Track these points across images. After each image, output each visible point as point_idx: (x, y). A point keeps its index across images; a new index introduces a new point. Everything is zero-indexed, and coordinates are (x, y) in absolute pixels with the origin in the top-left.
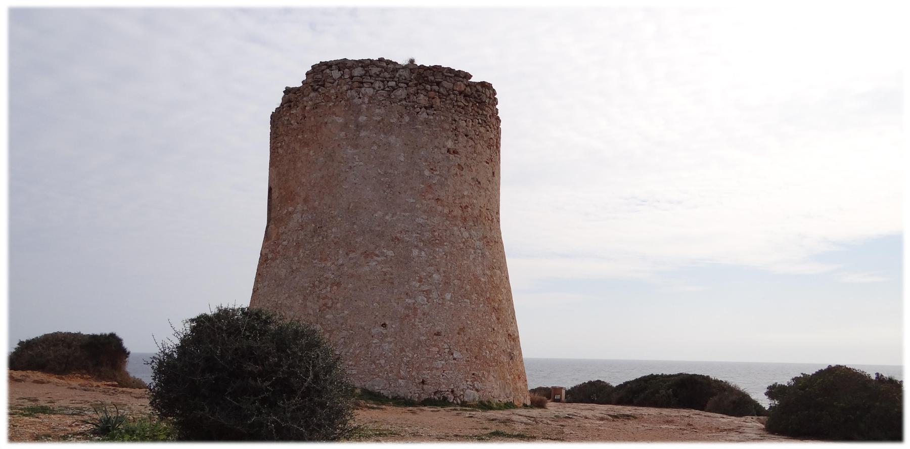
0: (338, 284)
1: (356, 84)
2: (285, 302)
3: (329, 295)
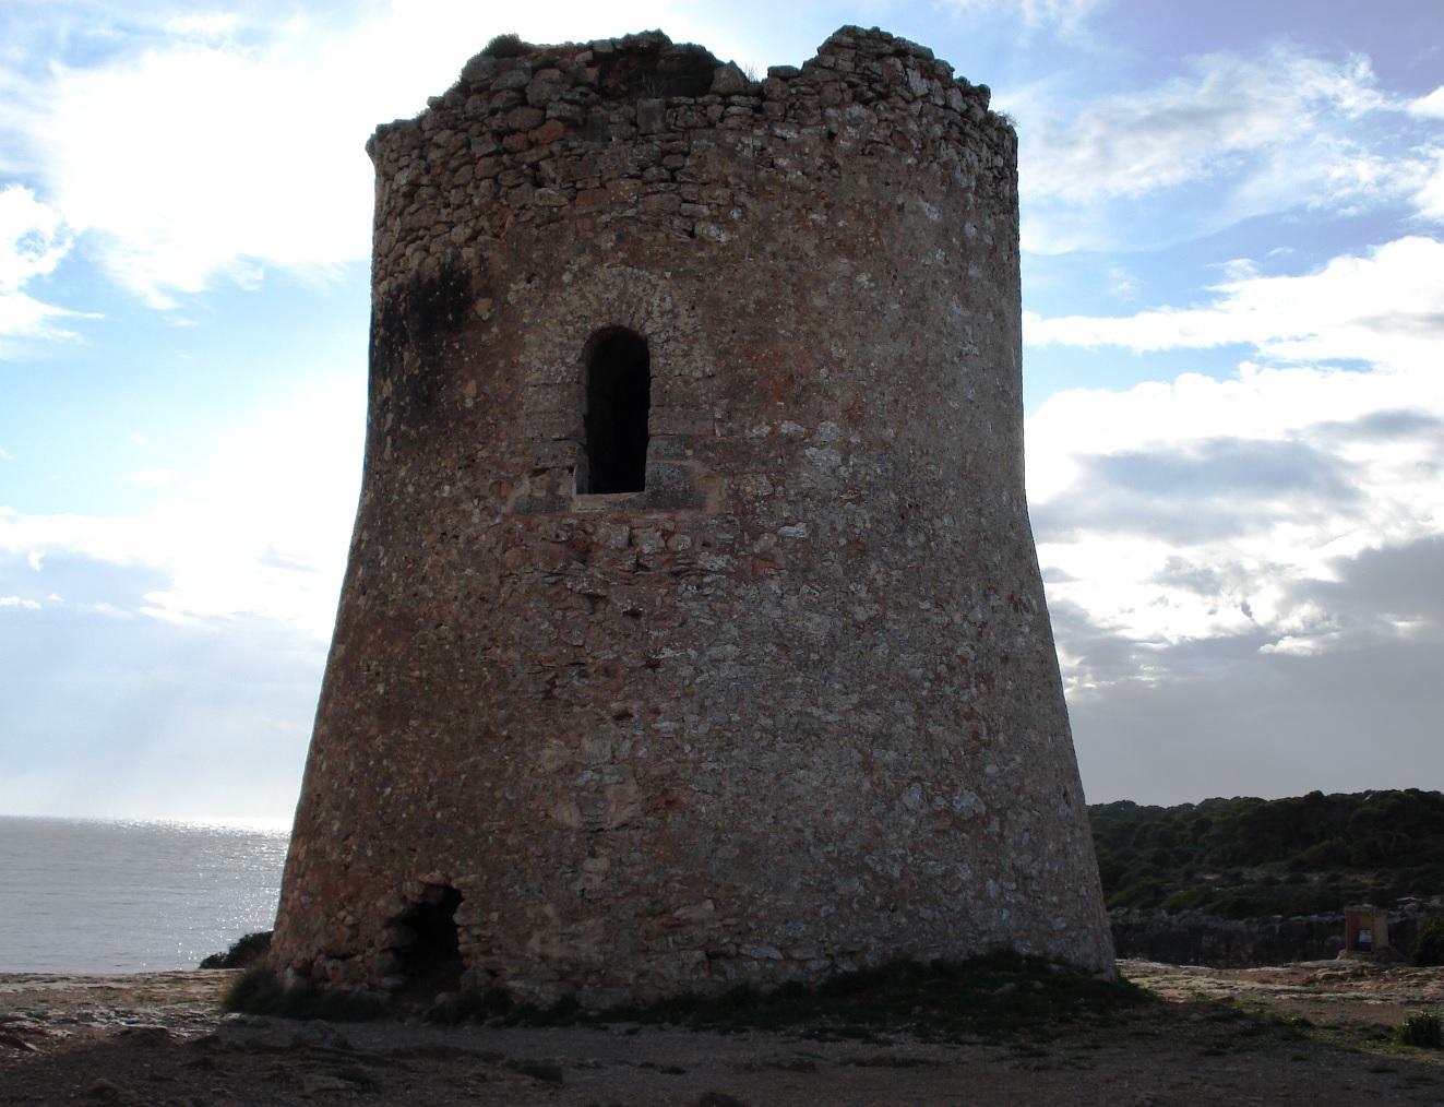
1: (955, 133)
2: (854, 719)
3: (978, 708)
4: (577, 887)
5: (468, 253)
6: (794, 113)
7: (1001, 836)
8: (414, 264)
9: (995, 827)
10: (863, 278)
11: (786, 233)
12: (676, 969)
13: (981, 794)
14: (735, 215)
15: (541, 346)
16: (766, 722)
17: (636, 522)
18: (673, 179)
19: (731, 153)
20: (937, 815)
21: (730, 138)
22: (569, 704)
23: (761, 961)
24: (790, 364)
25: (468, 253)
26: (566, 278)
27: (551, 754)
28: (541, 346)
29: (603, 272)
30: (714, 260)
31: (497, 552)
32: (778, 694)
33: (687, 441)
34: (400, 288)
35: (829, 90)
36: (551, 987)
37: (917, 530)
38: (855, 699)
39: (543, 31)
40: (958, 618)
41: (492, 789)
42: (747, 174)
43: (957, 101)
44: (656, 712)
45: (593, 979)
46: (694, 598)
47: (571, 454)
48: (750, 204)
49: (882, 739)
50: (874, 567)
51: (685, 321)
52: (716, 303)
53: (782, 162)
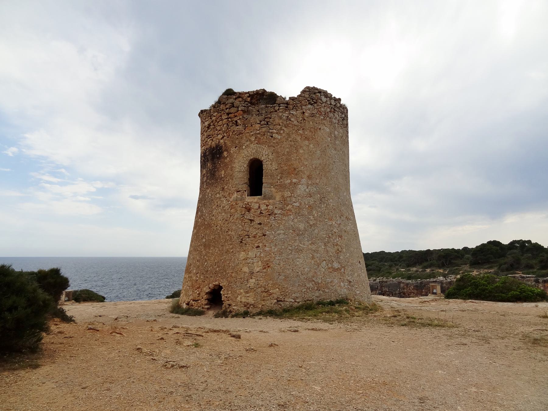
0: (341, 237)
1: (333, 110)
4: (248, 286)
5: (222, 141)
6: (295, 107)
7: (344, 273)
8: (210, 143)
9: (343, 270)
10: (311, 146)
11: (293, 136)
12: (270, 304)
13: (339, 263)
14: (282, 132)
15: (239, 163)
16: (291, 248)
17: (260, 203)
18: (268, 124)
19: (281, 118)
20: (329, 268)
21: (280, 114)
22: (246, 244)
23: (289, 301)
24: (295, 166)
25: (222, 141)
26: (244, 147)
27: (242, 255)
28: (239, 163)
29: (252, 146)
30: (277, 143)
31: (229, 210)
32: (293, 242)
33: (272, 184)
34: (207, 149)
35: (303, 102)
36: (242, 308)
37: (324, 203)
38: (310, 242)
39: (237, 89)
40: (334, 223)
41: (229, 263)
42: (285, 122)
43: (333, 103)
44: (265, 246)
45: (252, 306)
46: (274, 220)
47: (245, 187)
48: (285, 129)
49: (316, 251)
50: (314, 212)
51: (271, 157)
52: (278, 153)
53: (292, 119)
